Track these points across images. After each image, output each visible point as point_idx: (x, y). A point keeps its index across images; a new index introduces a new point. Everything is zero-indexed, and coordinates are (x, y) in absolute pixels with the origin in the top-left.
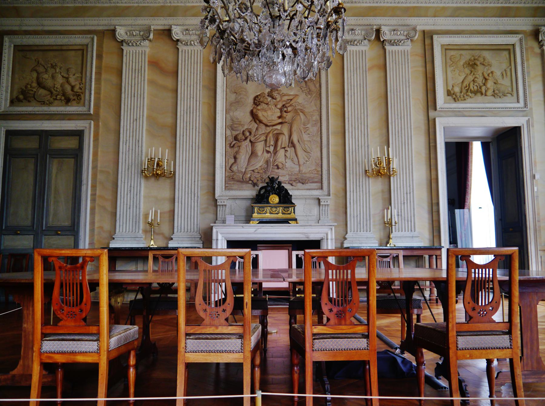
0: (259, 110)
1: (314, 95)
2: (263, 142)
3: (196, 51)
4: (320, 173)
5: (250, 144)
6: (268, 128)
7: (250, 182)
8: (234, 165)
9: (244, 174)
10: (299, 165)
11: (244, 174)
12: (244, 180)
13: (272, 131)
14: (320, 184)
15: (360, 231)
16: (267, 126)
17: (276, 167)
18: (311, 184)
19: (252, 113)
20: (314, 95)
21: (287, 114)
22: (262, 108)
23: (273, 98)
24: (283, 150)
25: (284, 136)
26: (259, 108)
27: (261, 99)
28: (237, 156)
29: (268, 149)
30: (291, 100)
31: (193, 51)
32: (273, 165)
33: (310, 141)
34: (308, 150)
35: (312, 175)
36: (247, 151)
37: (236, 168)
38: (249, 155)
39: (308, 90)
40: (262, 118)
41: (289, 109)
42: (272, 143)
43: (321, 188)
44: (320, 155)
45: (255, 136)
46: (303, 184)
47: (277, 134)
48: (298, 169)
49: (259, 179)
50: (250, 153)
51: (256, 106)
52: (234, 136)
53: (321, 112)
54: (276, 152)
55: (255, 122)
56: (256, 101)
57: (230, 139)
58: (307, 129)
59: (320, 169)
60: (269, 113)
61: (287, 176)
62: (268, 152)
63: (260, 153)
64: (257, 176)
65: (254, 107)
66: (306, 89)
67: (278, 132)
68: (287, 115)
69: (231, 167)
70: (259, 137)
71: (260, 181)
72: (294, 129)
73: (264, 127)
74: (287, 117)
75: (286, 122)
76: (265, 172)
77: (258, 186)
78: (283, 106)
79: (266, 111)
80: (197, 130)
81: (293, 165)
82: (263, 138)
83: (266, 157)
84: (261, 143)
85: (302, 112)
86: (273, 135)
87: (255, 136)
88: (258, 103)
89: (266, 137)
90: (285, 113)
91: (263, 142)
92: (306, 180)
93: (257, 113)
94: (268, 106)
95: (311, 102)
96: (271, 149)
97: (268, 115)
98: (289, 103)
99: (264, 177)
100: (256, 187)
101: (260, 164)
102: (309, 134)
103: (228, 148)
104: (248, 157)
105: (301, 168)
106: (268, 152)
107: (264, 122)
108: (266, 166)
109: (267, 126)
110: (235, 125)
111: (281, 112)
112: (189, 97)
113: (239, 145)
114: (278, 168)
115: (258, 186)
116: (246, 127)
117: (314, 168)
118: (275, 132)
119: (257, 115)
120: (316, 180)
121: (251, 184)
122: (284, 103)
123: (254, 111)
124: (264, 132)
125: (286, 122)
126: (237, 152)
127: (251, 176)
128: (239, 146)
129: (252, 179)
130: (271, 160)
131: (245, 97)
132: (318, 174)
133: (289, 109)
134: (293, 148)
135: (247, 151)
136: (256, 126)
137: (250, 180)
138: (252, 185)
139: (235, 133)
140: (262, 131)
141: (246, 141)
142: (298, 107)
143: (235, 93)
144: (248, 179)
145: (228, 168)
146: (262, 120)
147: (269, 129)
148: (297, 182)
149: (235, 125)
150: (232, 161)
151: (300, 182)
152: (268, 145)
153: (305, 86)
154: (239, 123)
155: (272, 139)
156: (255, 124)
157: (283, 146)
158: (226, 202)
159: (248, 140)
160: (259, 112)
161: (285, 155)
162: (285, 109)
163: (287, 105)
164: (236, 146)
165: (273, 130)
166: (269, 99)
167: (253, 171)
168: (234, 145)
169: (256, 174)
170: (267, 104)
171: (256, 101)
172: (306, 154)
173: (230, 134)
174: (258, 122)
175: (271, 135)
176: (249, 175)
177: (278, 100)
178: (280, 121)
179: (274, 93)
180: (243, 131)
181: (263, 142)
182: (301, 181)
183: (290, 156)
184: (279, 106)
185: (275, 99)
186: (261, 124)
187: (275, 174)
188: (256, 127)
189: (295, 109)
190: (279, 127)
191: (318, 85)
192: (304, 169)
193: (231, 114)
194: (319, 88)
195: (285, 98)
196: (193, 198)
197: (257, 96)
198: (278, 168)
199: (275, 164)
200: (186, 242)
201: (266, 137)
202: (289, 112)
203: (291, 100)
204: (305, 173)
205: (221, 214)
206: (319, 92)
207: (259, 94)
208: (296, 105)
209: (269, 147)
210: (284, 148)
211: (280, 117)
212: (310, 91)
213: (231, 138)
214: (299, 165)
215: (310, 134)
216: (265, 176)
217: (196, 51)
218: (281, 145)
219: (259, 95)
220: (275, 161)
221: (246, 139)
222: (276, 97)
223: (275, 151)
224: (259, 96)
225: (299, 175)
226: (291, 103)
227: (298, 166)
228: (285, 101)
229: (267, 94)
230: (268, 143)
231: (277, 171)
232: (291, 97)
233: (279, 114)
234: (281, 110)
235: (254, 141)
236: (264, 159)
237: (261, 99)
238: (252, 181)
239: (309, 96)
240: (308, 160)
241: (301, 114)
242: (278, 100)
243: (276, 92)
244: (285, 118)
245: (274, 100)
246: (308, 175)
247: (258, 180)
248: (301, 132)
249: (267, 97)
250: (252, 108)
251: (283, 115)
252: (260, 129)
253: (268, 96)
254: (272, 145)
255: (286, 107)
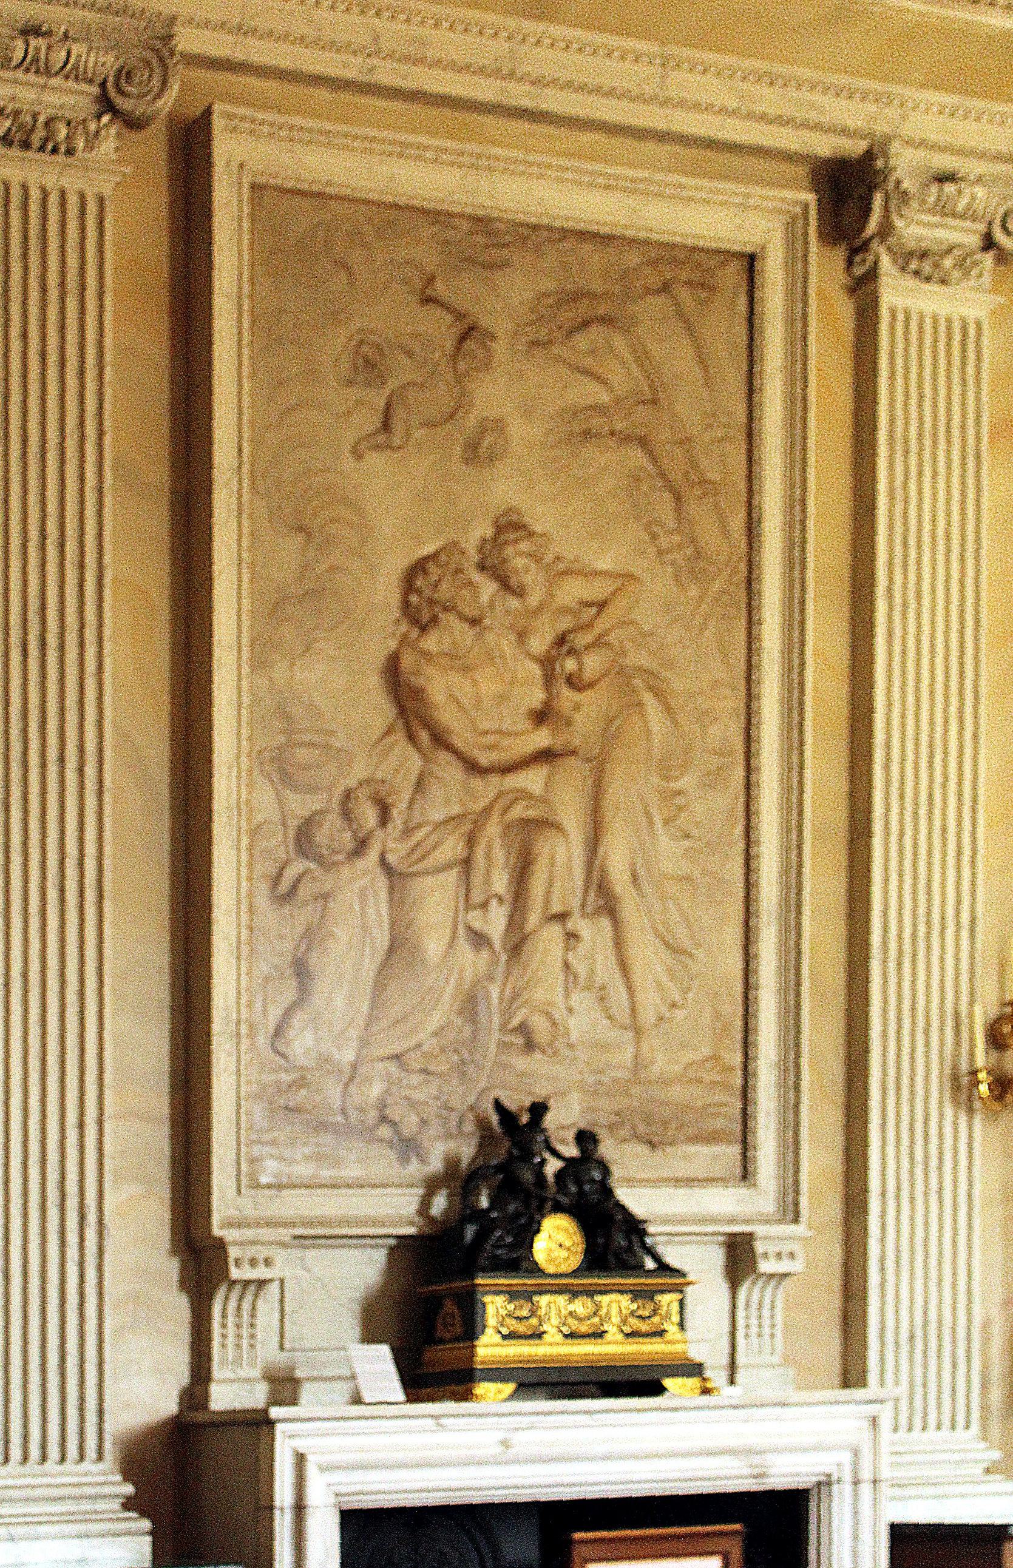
0: (427, 656)
1: (717, 585)
2: (454, 872)
3: (73, 201)
4: (738, 1081)
5: (382, 883)
6: (477, 783)
7: (385, 1131)
8: (297, 1021)
9: (351, 1079)
10: (638, 1031)
11: (351, 1079)
12: (354, 1116)
13: (498, 807)
14: (736, 1149)
15: (910, 1429)
16: (473, 767)
17: (519, 1040)
18: (692, 1149)
19: (393, 670)
20: (717, 585)
21: (577, 697)
22: (446, 647)
23: (506, 585)
24: (555, 931)
25: (559, 841)
26: (430, 643)
27: (445, 591)
28: (314, 959)
29: (475, 918)
30: (602, 605)
31: (53, 199)
32: (503, 1026)
33: (687, 878)
34: (682, 936)
35: (699, 1096)
36: (365, 929)
37: (308, 1039)
38: (379, 958)
39: (689, 551)
40: (447, 716)
41: (593, 664)
42: (501, 883)
43: (738, 1171)
44: (739, 965)
45: (408, 831)
46: (652, 1145)
47: (525, 823)
48: (627, 1055)
49: (432, 1111)
50: (382, 938)
51: (415, 634)
52: (293, 823)
53: (751, 697)
54: (524, 939)
55: (412, 737)
56: (414, 599)
57: (279, 844)
58: (680, 800)
59: (738, 1059)
60: (488, 685)
61: (575, 1096)
62: (479, 939)
63: (433, 946)
64: (417, 1095)
65: (404, 641)
66: (676, 538)
67: (532, 813)
68: (577, 707)
69: (278, 1032)
70: (432, 840)
71: (434, 1130)
72: (616, 792)
73: (450, 771)
74: (578, 717)
75: (573, 753)
76: (461, 1069)
77: (423, 1161)
78: (561, 640)
79: (466, 669)
80: (90, 770)
81: (605, 1031)
82: (451, 847)
83: (469, 974)
84: (441, 878)
85: (651, 688)
86: (508, 827)
87: (408, 831)
88: (425, 616)
89: (471, 841)
90: (566, 692)
91: (452, 876)
92: (665, 1124)
93: (420, 682)
94: (480, 636)
95: (703, 627)
96: (496, 922)
97: (478, 699)
98: (589, 626)
99: (455, 1101)
100: (414, 1161)
101: (435, 1020)
102: (687, 836)
103: (263, 901)
104: (370, 966)
105: (645, 1047)
106: (479, 939)
107: (458, 742)
108: (468, 1030)
109: (473, 767)
110: (302, 755)
111: (549, 680)
112: (34, 534)
113: (328, 887)
114: (530, 1046)
115: (423, 1161)
116: (359, 770)
117: (706, 1051)
118: (518, 811)
119: (418, 694)
120: (720, 1123)
121: (390, 1144)
122: (565, 623)
123: (407, 661)
124: (456, 810)
125: (573, 753)
126: (312, 936)
127: (387, 1092)
128: (325, 897)
129: (394, 1114)
130: (494, 991)
131: (356, 565)
132: (727, 1087)
133: (593, 664)
134: (605, 923)
135: (365, 929)
136: (416, 762)
137: (384, 1119)
138: (393, 1155)
139: (300, 805)
140: (447, 802)
141: (360, 864)
142: (638, 658)
143: (301, 529)
144: (372, 1115)
145: (262, 1041)
146: (448, 731)
147: (487, 788)
148: (623, 1133)
149: (302, 755)
150: (289, 992)
151: (636, 1136)
152: (477, 897)
153: (671, 524)
154: (317, 739)
155: (499, 855)
156: (411, 750)
157: (556, 908)
158: (278, 1261)
159: (372, 856)
160: (431, 671)
161: (567, 966)
162: (570, 665)
163: (582, 640)
164: (303, 892)
165: (505, 800)
166: (488, 588)
167: (397, 1057)
168: (294, 888)
169: (415, 1079)
170: (474, 622)
171: (414, 599)
172: (668, 957)
173: (276, 816)
174: (424, 736)
175: (493, 829)
176: (376, 1090)
177: (534, 600)
178: (542, 739)
179: (510, 550)
180: (348, 796)
181: (454, 872)
182: (642, 1128)
183: (592, 971)
184: (539, 644)
185: (519, 592)
186: (444, 756)
187: (512, 1079)
188: (413, 777)
189: (622, 672)
190: (533, 780)
191: (737, 523)
192: (661, 1064)
193: (279, 674)
194: (743, 545)
195: (572, 591)
196: (72, 1238)
197: (419, 567)
198: (530, 1046)
199: (515, 1022)
200: (56, 1529)
201: (471, 841)
202: (591, 685)
203: (602, 605)
204: (665, 1082)
205: (231, 1340)
206: (743, 567)
207: (429, 549)
208: (628, 645)
209: (484, 905)
210: (562, 917)
211: (541, 716)
212: (698, 554)
213: (280, 837)
214: (638, 1031)
215: (696, 833)
216: (461, 1097)
217: (73, 201)
218: (547, 901)
219: (434, 556)
220: (514, 998)
221: (361, 847)
222: (528, 579)
223: (516, 938)
224: (431, 567)
225: (636, 1090)
226: (601, 625)
227: (630, 1034)
228: (566, 610)
229: (475, 557)
230: (477, 879)
231: (521, 1063)
232: (597, 590)
233: (536, 697)
234: (547, 663)
235: (403, 868)
236: (458, 987)
237: (444, 585)
238: (393, 1124)
239: (694, 591)
240: (677, 998)
241: (648, 699)
242: (534, 600)
243: (524, 546)
244: (569, 723)
245: (514, 603)
246: (677, 1093)
247: (424, 1122)
248: (651, 823)
249: (477, 577)
250: (393, 644)
251: (555, 703)
252: (436, 791)
253: (482, 567)
254: (500, 900)
255: (572, 652)
